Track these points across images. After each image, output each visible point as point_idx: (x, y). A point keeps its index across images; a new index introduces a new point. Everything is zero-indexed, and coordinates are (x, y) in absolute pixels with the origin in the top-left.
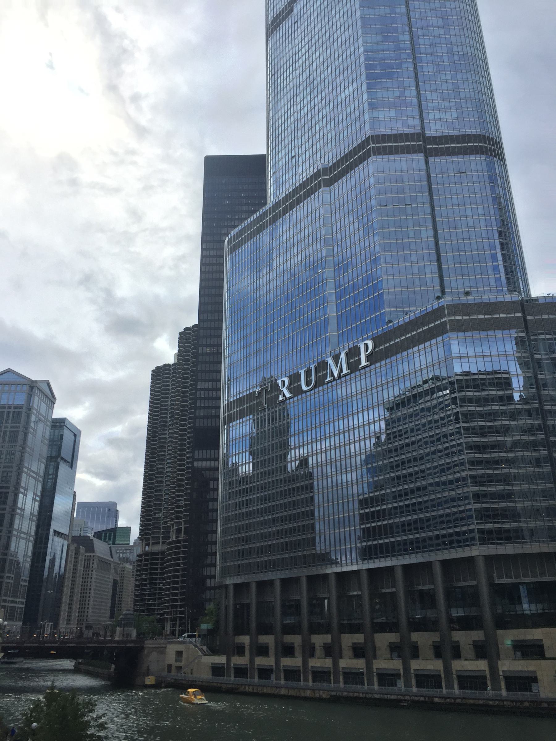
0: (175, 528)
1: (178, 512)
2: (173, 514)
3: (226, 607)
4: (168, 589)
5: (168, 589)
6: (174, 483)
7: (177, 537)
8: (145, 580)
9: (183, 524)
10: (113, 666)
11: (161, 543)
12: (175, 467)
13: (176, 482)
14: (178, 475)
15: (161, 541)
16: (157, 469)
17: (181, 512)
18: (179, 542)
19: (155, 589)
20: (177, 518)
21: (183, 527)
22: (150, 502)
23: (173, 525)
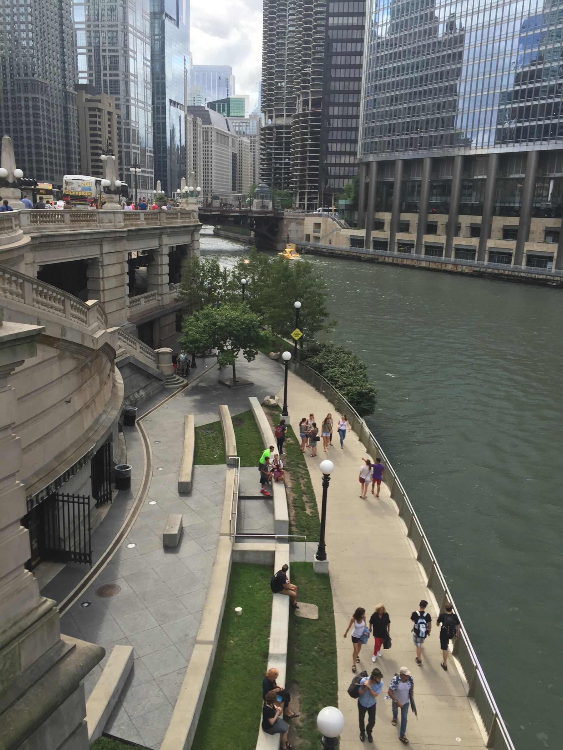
0: (301, 99)
1: (304, 81)
2: (299, 83)
3: (367, 185)
4: (296, 164)
5: (296, 164)
6: (299, 45)
7: (304, 110)
8: (270, 154)
9: (310, 95)
10: (253, 233)
12: (300, 26)
13: (301, 44)
14: (304, 35)
15: (285, 114)
16: (278, 27)
17: (308, 81)
19: (281, 164)
20: (304, 88)
21: (310, 98)
22: (271, 68)
23: (299, 96)
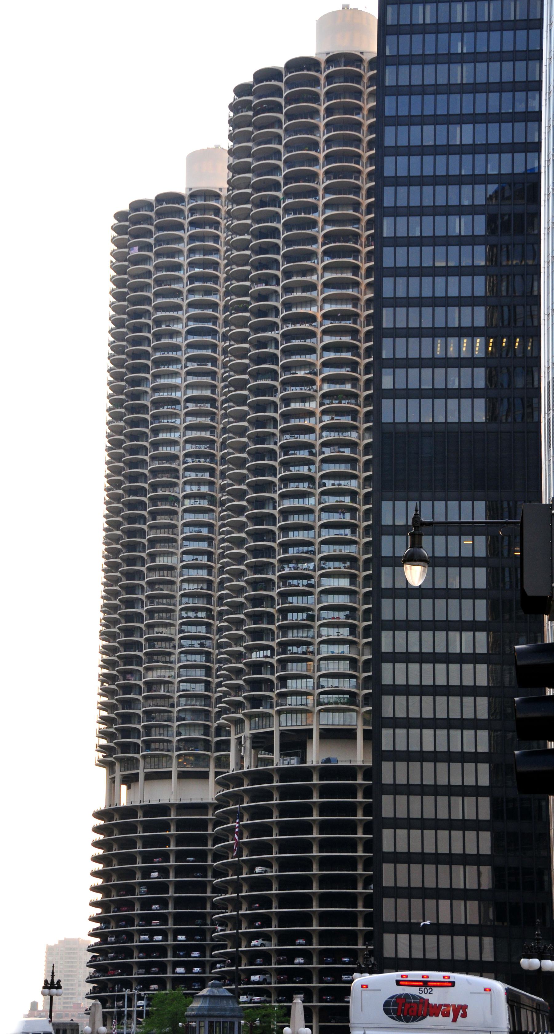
0: (248, 732)
11: (174, 775)
18: (266, 777)
23: (239, 723)
